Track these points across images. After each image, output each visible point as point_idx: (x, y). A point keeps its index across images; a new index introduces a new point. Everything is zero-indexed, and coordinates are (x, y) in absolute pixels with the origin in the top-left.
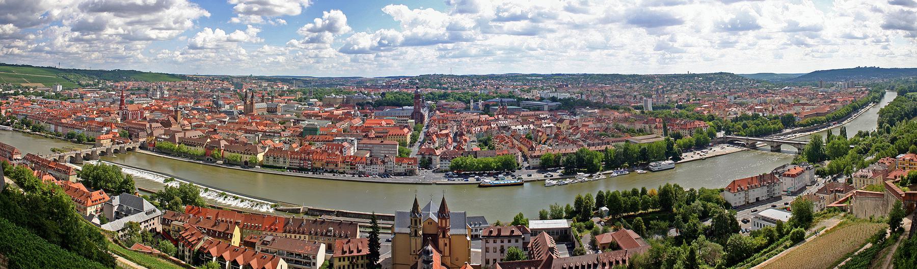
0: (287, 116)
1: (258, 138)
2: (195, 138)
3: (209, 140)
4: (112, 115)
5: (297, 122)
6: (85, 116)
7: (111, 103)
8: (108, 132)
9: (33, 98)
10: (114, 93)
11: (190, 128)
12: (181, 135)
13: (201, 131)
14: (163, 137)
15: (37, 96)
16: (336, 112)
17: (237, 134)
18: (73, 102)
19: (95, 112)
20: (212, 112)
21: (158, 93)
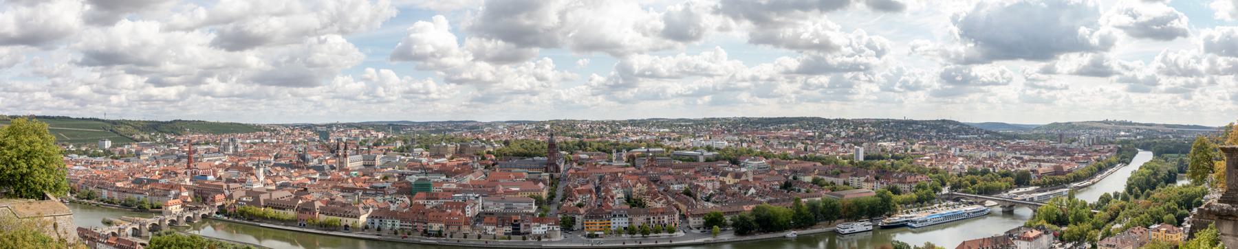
0: (389, 169)
3: (300, 202)
7: (175, 161)
9: (75, 156)
10: (177, 148)
11: (274, 188)
12: (266, 196)
13: (289, 191)
14: (244, 199)
15: (79, 155)
16: (449, 164)
17: (333, 193)
18: (128, 161)
19: (157, 172)
20: (298, 168)
21: (231, 147)
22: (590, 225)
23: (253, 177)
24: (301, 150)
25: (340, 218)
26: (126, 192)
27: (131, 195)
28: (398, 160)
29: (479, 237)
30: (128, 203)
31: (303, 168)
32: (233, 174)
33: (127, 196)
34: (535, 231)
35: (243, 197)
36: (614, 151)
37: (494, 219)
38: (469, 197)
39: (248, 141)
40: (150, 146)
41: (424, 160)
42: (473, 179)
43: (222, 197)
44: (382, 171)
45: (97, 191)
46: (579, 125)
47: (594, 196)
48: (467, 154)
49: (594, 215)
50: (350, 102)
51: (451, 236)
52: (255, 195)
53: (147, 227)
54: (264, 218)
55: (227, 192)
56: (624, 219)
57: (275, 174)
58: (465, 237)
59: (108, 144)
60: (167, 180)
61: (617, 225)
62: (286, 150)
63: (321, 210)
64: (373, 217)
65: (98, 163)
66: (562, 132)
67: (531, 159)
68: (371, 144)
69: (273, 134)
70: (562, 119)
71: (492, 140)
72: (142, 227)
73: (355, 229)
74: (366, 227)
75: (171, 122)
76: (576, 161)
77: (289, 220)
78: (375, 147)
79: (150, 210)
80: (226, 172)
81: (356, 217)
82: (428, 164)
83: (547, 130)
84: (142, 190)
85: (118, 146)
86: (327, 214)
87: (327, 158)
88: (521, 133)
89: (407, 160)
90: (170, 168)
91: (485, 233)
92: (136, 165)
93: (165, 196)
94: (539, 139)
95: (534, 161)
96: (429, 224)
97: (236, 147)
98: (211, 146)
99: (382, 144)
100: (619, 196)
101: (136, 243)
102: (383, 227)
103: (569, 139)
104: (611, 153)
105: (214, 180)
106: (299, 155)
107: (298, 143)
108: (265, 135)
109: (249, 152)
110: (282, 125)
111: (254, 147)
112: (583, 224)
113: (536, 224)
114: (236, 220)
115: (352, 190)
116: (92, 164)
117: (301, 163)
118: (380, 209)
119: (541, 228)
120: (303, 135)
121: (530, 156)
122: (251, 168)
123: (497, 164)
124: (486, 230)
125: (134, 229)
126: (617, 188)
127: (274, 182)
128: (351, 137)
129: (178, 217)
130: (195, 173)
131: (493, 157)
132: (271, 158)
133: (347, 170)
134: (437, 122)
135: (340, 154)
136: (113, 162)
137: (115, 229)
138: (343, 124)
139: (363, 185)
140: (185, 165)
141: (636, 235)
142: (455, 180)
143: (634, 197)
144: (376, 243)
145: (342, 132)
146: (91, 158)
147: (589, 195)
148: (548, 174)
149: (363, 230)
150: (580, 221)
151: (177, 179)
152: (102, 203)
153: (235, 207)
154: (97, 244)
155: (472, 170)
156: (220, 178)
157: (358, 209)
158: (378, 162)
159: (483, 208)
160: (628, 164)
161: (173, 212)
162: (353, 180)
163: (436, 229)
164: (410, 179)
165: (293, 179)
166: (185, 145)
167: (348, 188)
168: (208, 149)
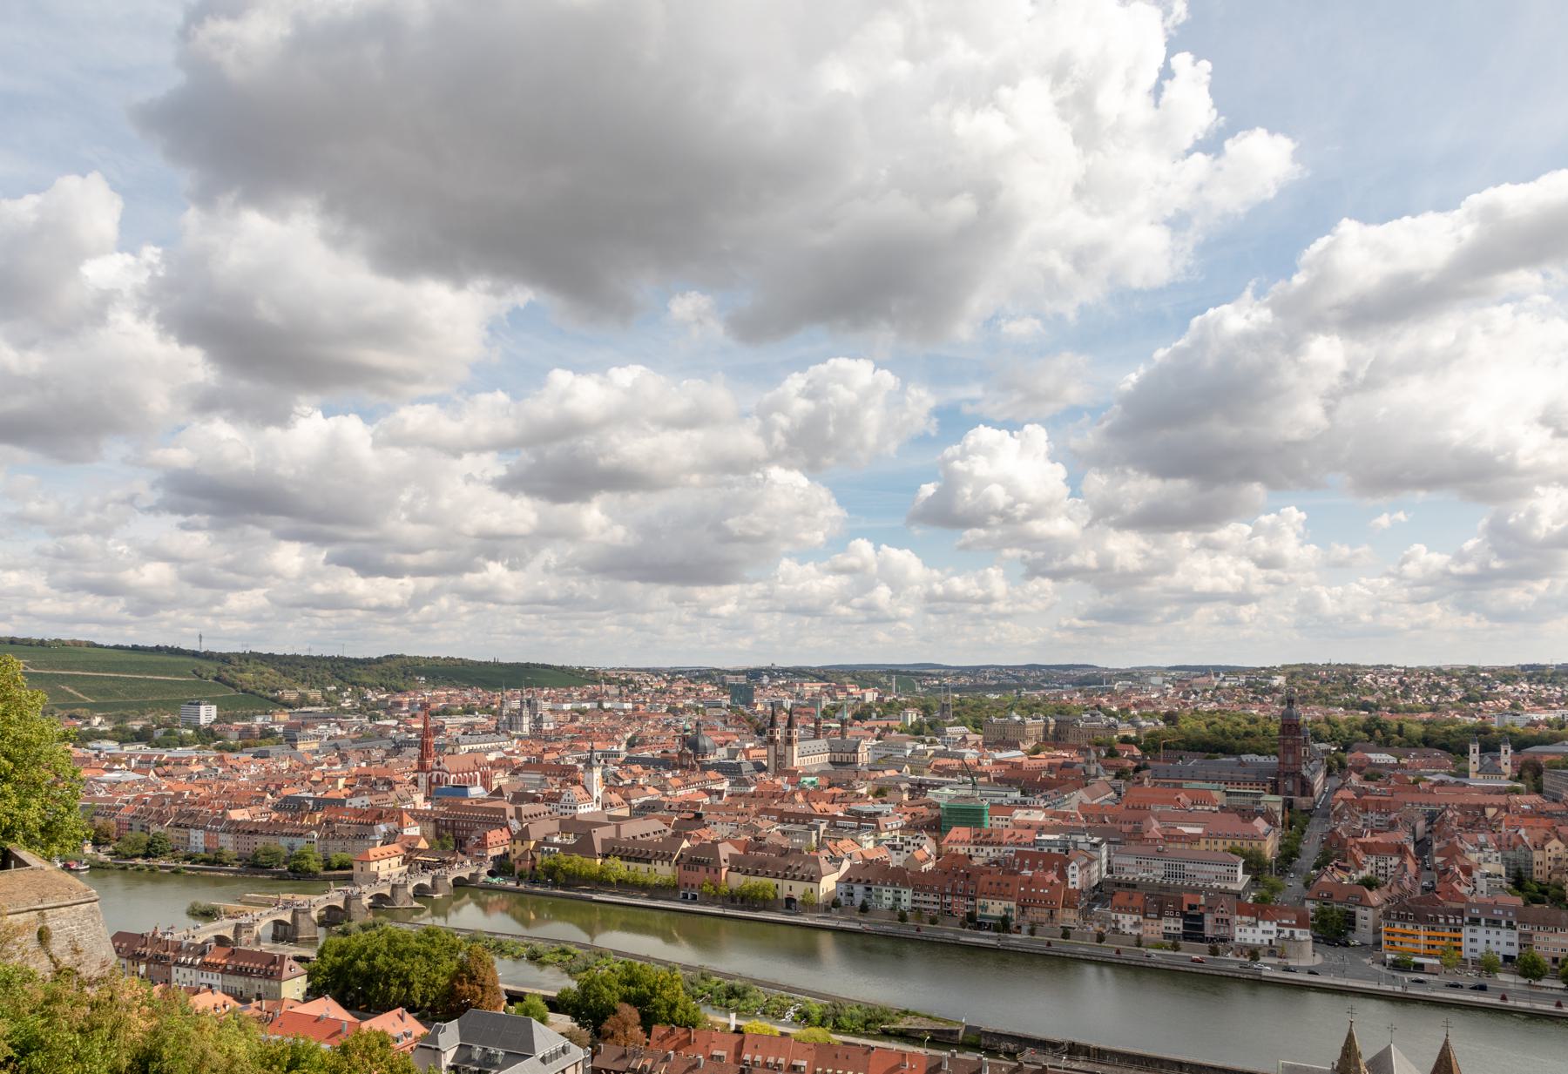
0: (888, 773)
1: (818, 834)
2: (646, 838)
4: (397, 787)
5: (918, 788)
6: (311, 795)
7: (388, 755)
8: (389, 839)
9: (110, 746)
10: (394, 723)
13: (661, 819)
14: (556, 839)
15: (122, 742)
16: (1028, 763)
17: (760, 824)
18: (264, 755)
19: (341, 782)
20: (682, 767)
21: (526, 720)
22: (1398, 938)
23: (577, 789)
24: (688, 727)
25: (775, 881)
26: (256, 832)
27: (271, 840)
28: (909, 752)
29: (1101, 938)
30: (262, 859)
31: (693, 768)
32: (531, 781)
33: (261, 842)
34: (1243, 935)
35: (553, 834)
36: (1474, 748)
37: (1137, 901)
38: (1076, 843)
39: (567, 707)
40: (325, 718)
41: (971, 755)
42: (1087, 800)
43: (505, 835)
44: (873, 776)
45: (174, 834)
46: (1368, 678)
47: (1410, 862)
48: (1071, 741)
49: (1410, 910)
50: (807, 620)
51: (1032, 932)
52: (582, 831)
53: (314, 915)
54: (601, 882)
55: (515, 825)
56: (1504, 932)
57: (628, 782)
58: (1066, 934)
59: (207, 714)
60: (367, 800)
61: (1481, 947)
62: (655, 727)
63: (732, 863)
64: (850, 880)
65: (178, 762)
66: (1318, 695)
67: (1234, 759)
68: (848, 716)
69: (626, 691)
70: (1320, 661)
71: (1134, 712)
72: (300, 916)
73: (809, 906)
74: (836, 904)
75: (379, 661)
76: (1359, 770)
77: (658, 886)
78: (857, 722)
79: (323, 873)
80: (515, 778)
81: (811, 880)
82: (979, 763)
83: (1276, 690)
84: (302, 827)
85: (235, 717)
86: (747, 873)
87: (748, 746)
88: (1208, 695)
89: (930, 753)
90: (376, 771)
91: (1116, 930)
92: (285, 765)
93: (361, 837)
94: (1255, 712)
95: (1242, 764)
96: (980, 901)
97: (538, 721)
98: (479, 718)
99: (874, 715)
100: (1487, 869)
101: (282, 957)
102: (872, 904)
103: (1339, 713)
104: (1464, 753)
105: (485, 796)
106: (684, 738)
107: (682, 711)
108: (606, 693)
109: (569, 731)
110: (647, 670)
111: (581, 719)
112: (1377, 932)
113: (1246, 919)
114: (537, 889)
115: (805, 818)
116: (158, 764)
117: (690, 756)
118: (868, 864)
119: (1259, 931)
120: (693, 694)
121: (1228, 750)
122: (574, 769)
123: (1146, 767)
124: (1117, 922)
125: (277, 923)
126: (1481, 847)
127: (627, 799)
128: (802, 698)
129: (394, 886)
130: (438, 782)
131: (1137, 752)
132: (619, 744)
133: (793, 775)
134: (1001, 667)
135: (778, 737)
136: (221, 759)
137: (225, 928)
138: (785, 670)
139: (829, 807)
140: (415, 761)
141: (1544, 982)
142: (1042, 803)
143: (1537, 877)
144: (855, 938)
145: (783, 687)
146: (158, 751)
147: (1396, 861)
148: (1279, 798)
149: (827, 910)
150: (1370, 922)
151: (393, 795)
152: (188, 864)
153: (533, 859)
154: (174, 969)
155: (1083, 781)
156: (499, 792)
157: (816, 861)
158: (864, 756)
159: (1110, 871)
160: (1519, 785)
161: (382, 875)
162: (806, 796)
163: (997, 914)
164: (937, 796)
165: (669, 793)
166: (413, 716)
167: (793, 814)
168: (471, 726)
